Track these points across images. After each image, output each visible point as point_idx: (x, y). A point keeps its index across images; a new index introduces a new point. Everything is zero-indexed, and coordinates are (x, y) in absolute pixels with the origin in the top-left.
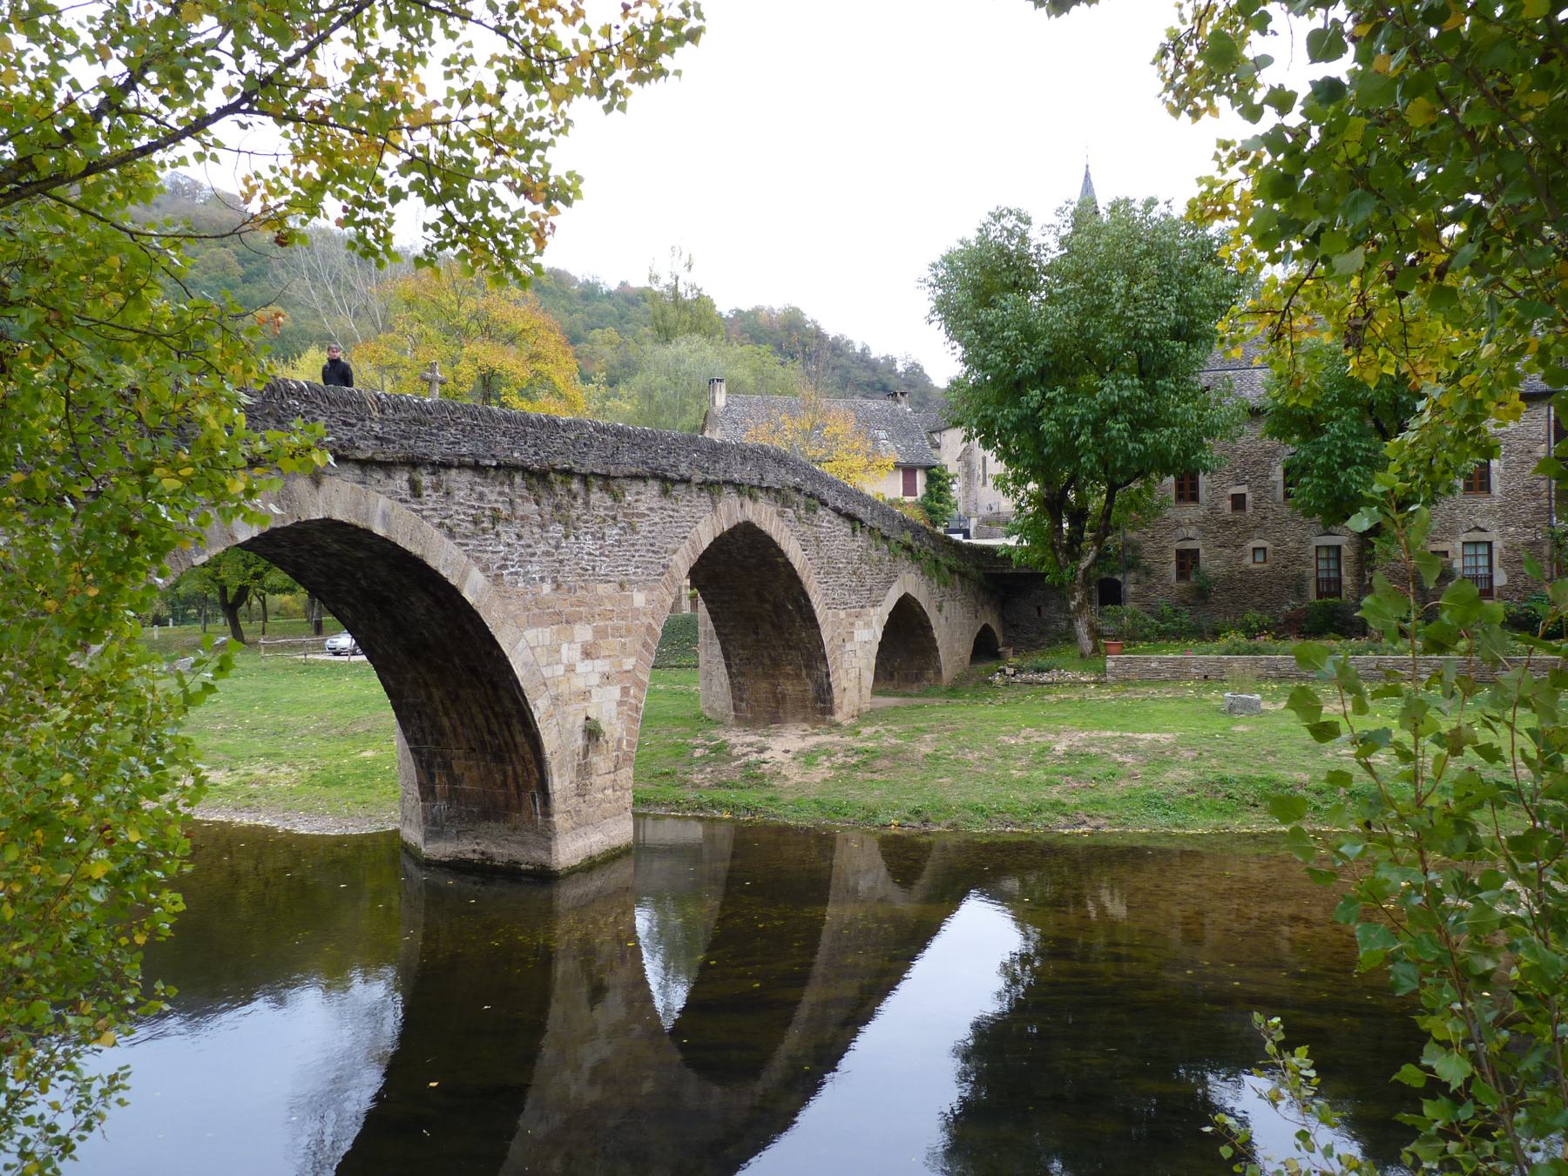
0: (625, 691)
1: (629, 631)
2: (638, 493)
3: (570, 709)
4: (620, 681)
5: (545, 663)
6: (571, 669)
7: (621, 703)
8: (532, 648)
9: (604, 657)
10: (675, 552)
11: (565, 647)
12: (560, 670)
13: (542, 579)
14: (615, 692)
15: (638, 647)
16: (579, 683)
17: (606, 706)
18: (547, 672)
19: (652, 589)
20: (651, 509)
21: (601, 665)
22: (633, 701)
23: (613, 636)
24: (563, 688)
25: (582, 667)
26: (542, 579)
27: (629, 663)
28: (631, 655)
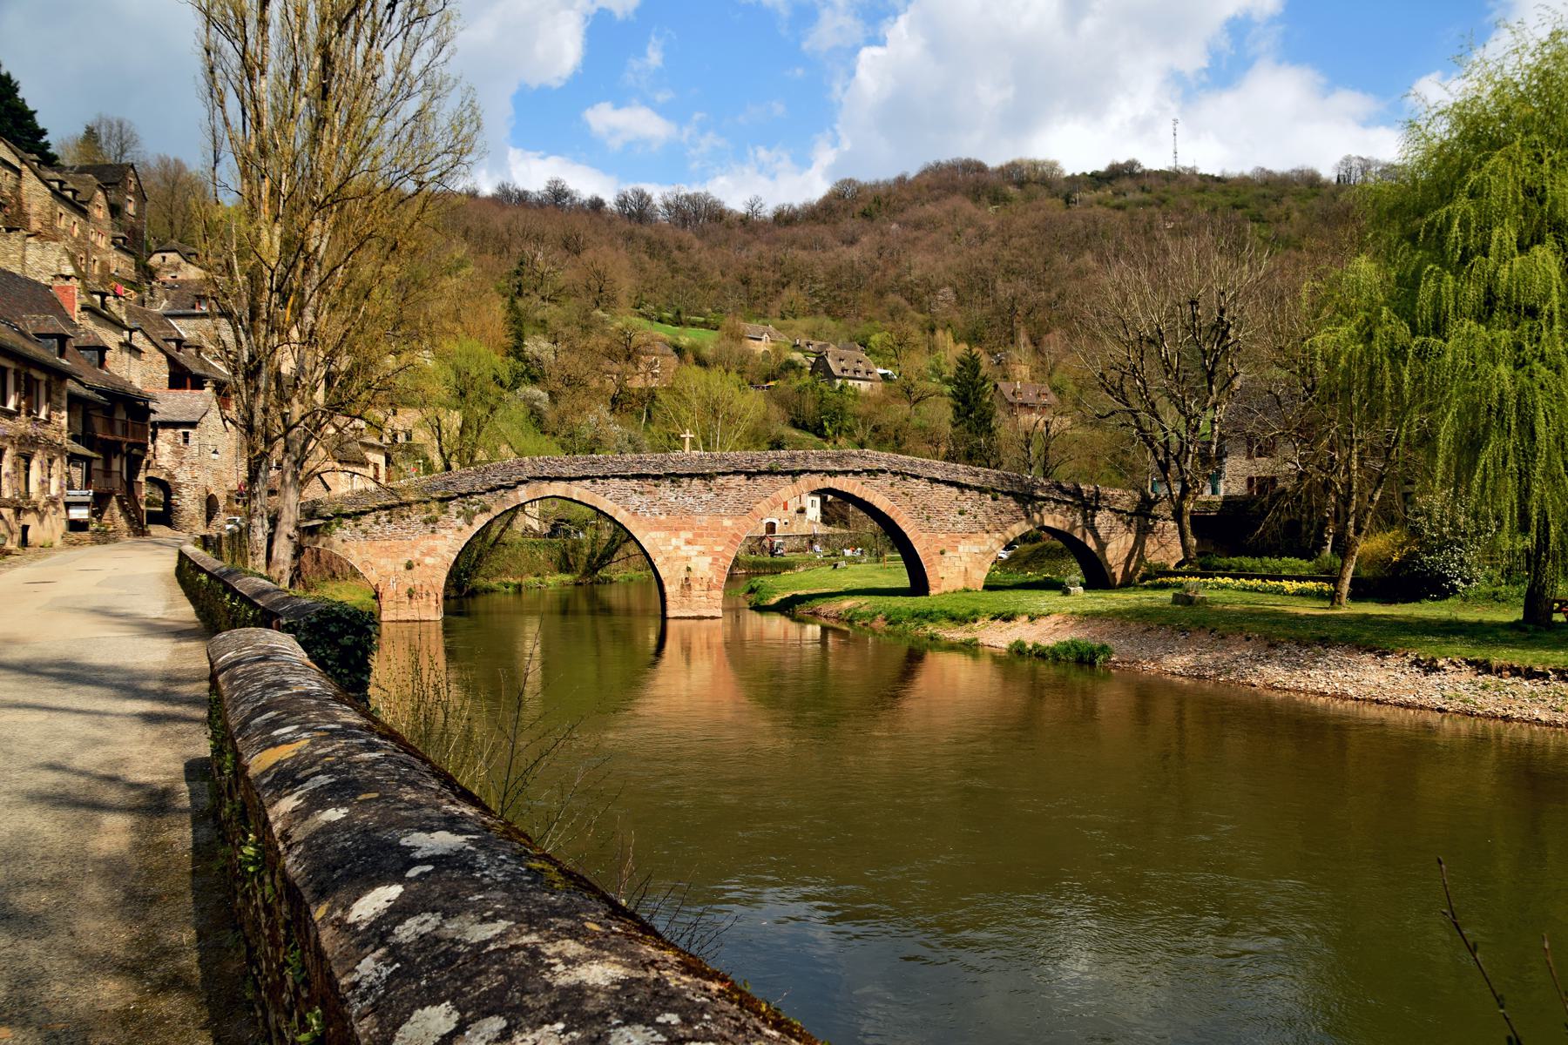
0: (716, 560)
1: (719, 536)
14: (709, 559)
16: (684, 554)
18: (662, 548)
27: (719, 549)
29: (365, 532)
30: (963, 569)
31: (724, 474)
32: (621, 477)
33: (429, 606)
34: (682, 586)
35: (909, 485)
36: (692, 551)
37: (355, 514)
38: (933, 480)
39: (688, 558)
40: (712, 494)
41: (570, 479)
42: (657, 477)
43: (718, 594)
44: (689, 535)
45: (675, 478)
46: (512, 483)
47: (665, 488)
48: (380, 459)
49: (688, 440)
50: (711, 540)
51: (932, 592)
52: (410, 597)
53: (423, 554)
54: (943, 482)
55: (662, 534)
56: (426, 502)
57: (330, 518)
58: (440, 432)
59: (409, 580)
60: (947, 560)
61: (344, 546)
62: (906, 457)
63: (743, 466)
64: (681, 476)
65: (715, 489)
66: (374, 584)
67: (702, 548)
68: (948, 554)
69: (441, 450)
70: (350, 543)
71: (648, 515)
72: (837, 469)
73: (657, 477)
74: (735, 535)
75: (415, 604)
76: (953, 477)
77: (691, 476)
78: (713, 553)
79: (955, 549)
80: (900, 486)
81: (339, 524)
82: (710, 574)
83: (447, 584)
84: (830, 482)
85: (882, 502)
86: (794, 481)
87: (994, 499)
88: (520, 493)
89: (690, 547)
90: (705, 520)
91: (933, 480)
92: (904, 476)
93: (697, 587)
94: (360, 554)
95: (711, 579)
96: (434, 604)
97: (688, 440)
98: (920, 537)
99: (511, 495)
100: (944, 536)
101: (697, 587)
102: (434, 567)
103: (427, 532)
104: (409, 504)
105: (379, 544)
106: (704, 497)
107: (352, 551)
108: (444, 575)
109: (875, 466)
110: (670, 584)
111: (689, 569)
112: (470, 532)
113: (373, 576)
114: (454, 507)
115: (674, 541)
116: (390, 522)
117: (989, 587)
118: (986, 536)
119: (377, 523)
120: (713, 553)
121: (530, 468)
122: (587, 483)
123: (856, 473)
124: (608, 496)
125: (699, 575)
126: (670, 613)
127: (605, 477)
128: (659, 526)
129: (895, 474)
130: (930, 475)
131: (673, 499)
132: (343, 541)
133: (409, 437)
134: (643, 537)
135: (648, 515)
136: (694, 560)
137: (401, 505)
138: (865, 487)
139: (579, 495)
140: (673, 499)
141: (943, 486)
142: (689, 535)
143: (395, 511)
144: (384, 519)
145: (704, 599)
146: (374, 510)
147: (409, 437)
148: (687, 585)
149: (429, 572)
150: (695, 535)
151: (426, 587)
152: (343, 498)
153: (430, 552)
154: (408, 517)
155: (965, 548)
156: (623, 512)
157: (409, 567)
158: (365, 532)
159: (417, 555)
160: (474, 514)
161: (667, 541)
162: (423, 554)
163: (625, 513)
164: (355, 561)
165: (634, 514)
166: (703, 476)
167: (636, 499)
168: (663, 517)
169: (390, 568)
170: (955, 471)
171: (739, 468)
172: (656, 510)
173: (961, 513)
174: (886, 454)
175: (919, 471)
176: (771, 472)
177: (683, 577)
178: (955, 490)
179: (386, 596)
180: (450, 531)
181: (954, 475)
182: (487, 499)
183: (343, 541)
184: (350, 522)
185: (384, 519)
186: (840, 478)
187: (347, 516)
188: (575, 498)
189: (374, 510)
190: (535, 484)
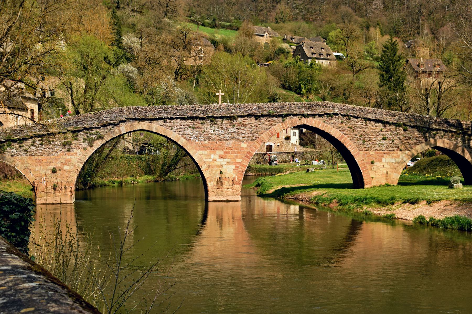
0: (237, 167)
1: (239, 153)
2: (245, 120)
3: (214, 169)
4: (234, 164)
5: (205, 158)
7: (234, 170)
8: (201, 155)
9: (229, 158)
10: (262, 134)
11: (212, 156)
12: (211, 160)
13: (205, 140)
14: (233, 167)
15: (243, 157)
16: (219, 164)
18: (206, 160)
19: (250, 143)
20: (250, 123)
21: (226, 160)
22: (241, 170)
23: (232, 154)
24: (212, 164)
28: (240, 158)
29: (26, 150)
30: (385, 172)
31: (242, 117)
32: (182, 118)
33: (66, 195)
34: (217, 183)
35: (352, 122)
36: (223, 162)
37: (19, 139)
38: (367, 119)
39: (221, 166)
40: (235, 129)
41: (151, 120)
42: (202, 119)
43: (238, 187)
44: (222, 153)
45: (213, 119)
46: (116, 122)
47: (207, 126)
48: (35, 107)
49: (220, 97)
51: (366, 186)
52: (55, 189)
53: (63, 164)
55: (206, 152)
56: (64, 133)
57: (4, 142)
58: (72, 91)
61: (12, 159)
62: (351, 106)
63: (253, 112)
64: (216, 118)
65: (236, 126)
66: (32, 181)
67: (229, 160)
68: (376, 163)
69: (73, 102)
70: (17, 157)
71: (197, 141)
72: (309, 113)
73: (202, 119)
74: (248, 153)
75: (57, 193)
76: (379, 117)
77: (222, 118)
78: (235, 163)
79: (380, 160)
80: (347, 123)
81: (9, 146)
82: (234, 175)
83: (77, 181)
84: (305, 121)
85: (335, 133)
86: (283, 121)
87: (405, 130)
88: (121, 128)
89: (222, 160)
90: (231, 144)
91: (367, 119)
92: (349, 117)
93: (226, 183)
94: (22, 164)
95: (234, 178)
96: (69, 193)
97: (220, 97)
98: (359, 153)
99: (116, 129)
100: (373, 153)
101: (226, 183)
102: (69, 171)
103: (65, 150)
104: (54, 134)
105: (36, 157)
106: (230, 130)
107: (18, 162)
108: (75, 176)
109: (332, 111)
110: (210, 181)
111: (221, 173)
112: (91, 151)
113: (31, 177)
114: (81, 136)
115: (212, 156)
116: (41, 144)
117: (399, 184)
118: (400, 152)
119: (33, 145)
120: (235, 163)
121: (127, 113)
122: (161, 122)
123: (320, 116)
124: (174, 130)
125: (227, 176)
126: (210, 198)
127: (172, 118)
128: (204, 148)
129: (344, 116)
130: (365, 116)
131: (212, 132)
132: (12, 156)
133: (52, 94)
134: (194, 154)
135: (197, 141)
137: (48, 134)
138: (325, 124)
139: (156, 129)
140: (212, 132)
141: (373, 123)
142: (222, 153)
143: (45, 138)
144: (38, 143)
145: (231, 190)
146: (32, 137)
147: (52, 94)
148: (220, 182)
149: (66, 174)
150: (225, 152)
151: (64, 184)
152: (11, 129)
153: (67, 162)
154: (53, 141)
156: (182, 139)
157: (54, 171)
158: (26, 150)
159: (59, 164)
160: (94, 140)
161: (208, 156)
162: (63, 164)
163: (184, 140)
164: (20, 168)
165: (189, 140)
166: (229, 118)
167: (190, 131)
168: (206, 142)
169: (42, 172)
170: (381, 113)
171: (251, 113)
172: (202, 138)
173: (384, 139)
174: (338, 104)
175: (358, 114)
176: (269, 115)
177: (218, 177)
178: (380, 125)
179: (40, 188)
180: (79, 150)
181: (380, 116)
182: (102, 131)
183: (12, 156)
184: (16, 145)
185: (38, 143)
186: (311, 118)
187: (14, 141)
188: (154, 131)
189: (32, 137)
190: (130, 123)
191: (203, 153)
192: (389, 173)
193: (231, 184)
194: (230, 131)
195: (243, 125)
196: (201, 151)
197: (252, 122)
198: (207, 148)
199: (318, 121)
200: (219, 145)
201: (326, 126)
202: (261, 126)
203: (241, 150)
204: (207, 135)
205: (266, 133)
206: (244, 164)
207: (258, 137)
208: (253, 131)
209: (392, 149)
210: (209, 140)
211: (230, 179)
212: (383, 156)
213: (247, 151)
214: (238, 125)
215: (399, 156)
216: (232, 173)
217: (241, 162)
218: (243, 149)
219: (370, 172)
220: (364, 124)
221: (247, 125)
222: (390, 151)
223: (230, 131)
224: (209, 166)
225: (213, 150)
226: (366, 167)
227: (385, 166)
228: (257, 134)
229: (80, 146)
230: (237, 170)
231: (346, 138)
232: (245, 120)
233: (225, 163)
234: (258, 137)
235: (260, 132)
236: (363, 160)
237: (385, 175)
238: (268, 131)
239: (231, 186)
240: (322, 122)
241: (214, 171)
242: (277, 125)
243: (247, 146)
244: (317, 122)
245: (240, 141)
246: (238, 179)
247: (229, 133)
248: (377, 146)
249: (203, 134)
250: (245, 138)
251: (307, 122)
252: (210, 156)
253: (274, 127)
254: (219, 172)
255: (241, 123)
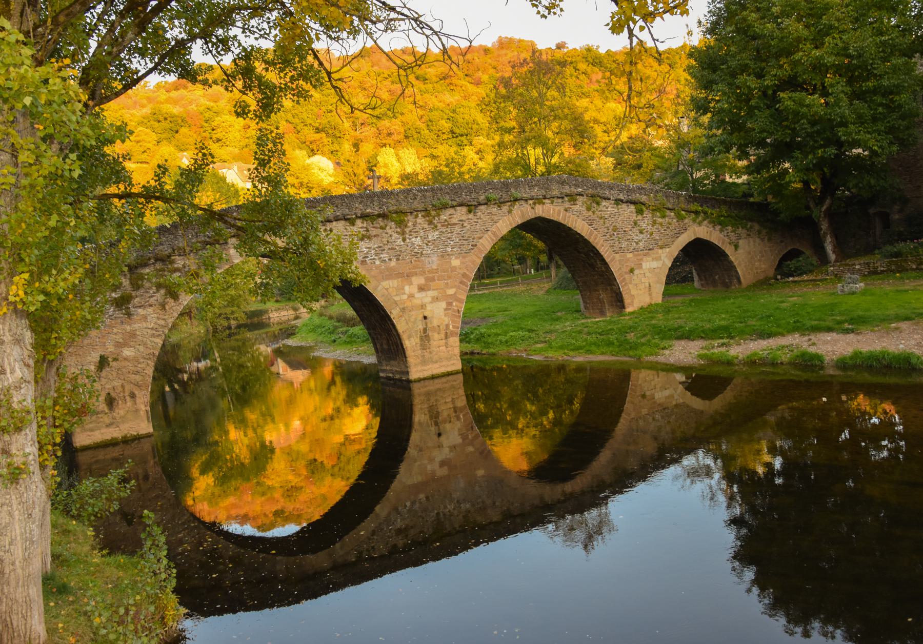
0: (449, 304)
1: (450, 277)
3: (413, 313)
6: (411, 296)
7: (446, 310)
8: (387, 289)
9: (434, 290)
10: (480, 238)
12: (405, 297)
13: (390, 260)
14: (443, 305)
15: (457, 284)
16: (417, 302)
17: (438, 312)
18: (397, 298)
19: (464, 257)
21: (431, 293)
22: (456, 308)
23: (438, 280)
24: (408, 304)
25: (418, 295)
26: (390, 260)
27: (451, 292)
28: (452, 287)
30: (647, 285)
34: (421, 339)
36: (425, 297)
39: (423, 306)
40: (437, 233)
50: (442, 283)
51: (629, 309)
53: (119, 345)
54: (627, 202)
59: (109, 382)
60: (635, 277)
65: (439, 225)
68: (636, 272)
71: (378, 262)
74: (464, 275)
82: (446, 320)
89: (423, 294)
91: (618, 201)
95: (447, 326)
98: (614, 258)
102: (136, 360)
106: (433, 235)
110: (409, 337)
118: (660, 251)
125: (435, 323)
128: (391, 274)
135: (378, 262)
136: (429, 307)
138: (568, 214)
141: (624, 206)
148: (425, 337)
150: (427, 279)
155: (649, 264)
159: (111, 348)
161: (400, 290)
168: (393, 263)
172: (384, 256)
177: (421, 327)
180: (150, 310)
191: (391, 284)
192: (652, 284)
193: (443, 336)
194: (430, 238)
195: (451, 225)
196: (387, 282)
197: (463, 218)
198: (395, 274)
199: (557, 208)
200: (415, 267)
201: (569, 217)
202: (478, 225)
203: (452, 271)
204: (392, 249)
205: (486, 236)
206: (459, 296)
207: (476, 245)
208: (467, 235)
209: (651, 247)
210: (398, 259)
211: (441, 327)
212: (641, 259)
213: (462, 272)
214: (443, 226)
215: (660, 257)
216: (443, 317)
217: (455, 293)
218: (454, 269)
219: (630, 285)
220: (616, 210)
221: (456, 224)
222: (650, 250)
223: (430, 238)
224: (404, 309)
225: (407, 276)
226: (624, 279)
227: (646, 275)
228: (474, 239)
229: (152, 300)
230: (450, 309)
231: (597, 235)
232: (450, 215)
233: (429, 299)
234: (476, 245)
235: (478, 235)
236: (620, 268)
237: (647, 289)
238: (489, 233)
239: (444, 341)
240: (562, 210)
241: (413, 317)
242: (501, 221)
243: (461, 263)
244: (556, 211)
245: (448, 255)
246: (454, 327)
247: (429, 242)
248: (634, 244)
249: (386, 247)
250: (455, 249)
251: (543, 212)
252: (403, 289)
253: (498, 224)
254: (421, 316)
255: (446, 220)
